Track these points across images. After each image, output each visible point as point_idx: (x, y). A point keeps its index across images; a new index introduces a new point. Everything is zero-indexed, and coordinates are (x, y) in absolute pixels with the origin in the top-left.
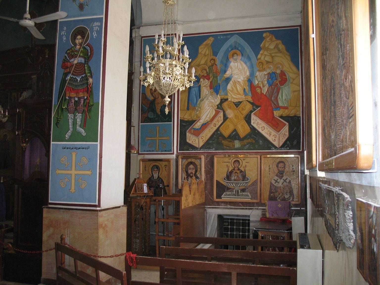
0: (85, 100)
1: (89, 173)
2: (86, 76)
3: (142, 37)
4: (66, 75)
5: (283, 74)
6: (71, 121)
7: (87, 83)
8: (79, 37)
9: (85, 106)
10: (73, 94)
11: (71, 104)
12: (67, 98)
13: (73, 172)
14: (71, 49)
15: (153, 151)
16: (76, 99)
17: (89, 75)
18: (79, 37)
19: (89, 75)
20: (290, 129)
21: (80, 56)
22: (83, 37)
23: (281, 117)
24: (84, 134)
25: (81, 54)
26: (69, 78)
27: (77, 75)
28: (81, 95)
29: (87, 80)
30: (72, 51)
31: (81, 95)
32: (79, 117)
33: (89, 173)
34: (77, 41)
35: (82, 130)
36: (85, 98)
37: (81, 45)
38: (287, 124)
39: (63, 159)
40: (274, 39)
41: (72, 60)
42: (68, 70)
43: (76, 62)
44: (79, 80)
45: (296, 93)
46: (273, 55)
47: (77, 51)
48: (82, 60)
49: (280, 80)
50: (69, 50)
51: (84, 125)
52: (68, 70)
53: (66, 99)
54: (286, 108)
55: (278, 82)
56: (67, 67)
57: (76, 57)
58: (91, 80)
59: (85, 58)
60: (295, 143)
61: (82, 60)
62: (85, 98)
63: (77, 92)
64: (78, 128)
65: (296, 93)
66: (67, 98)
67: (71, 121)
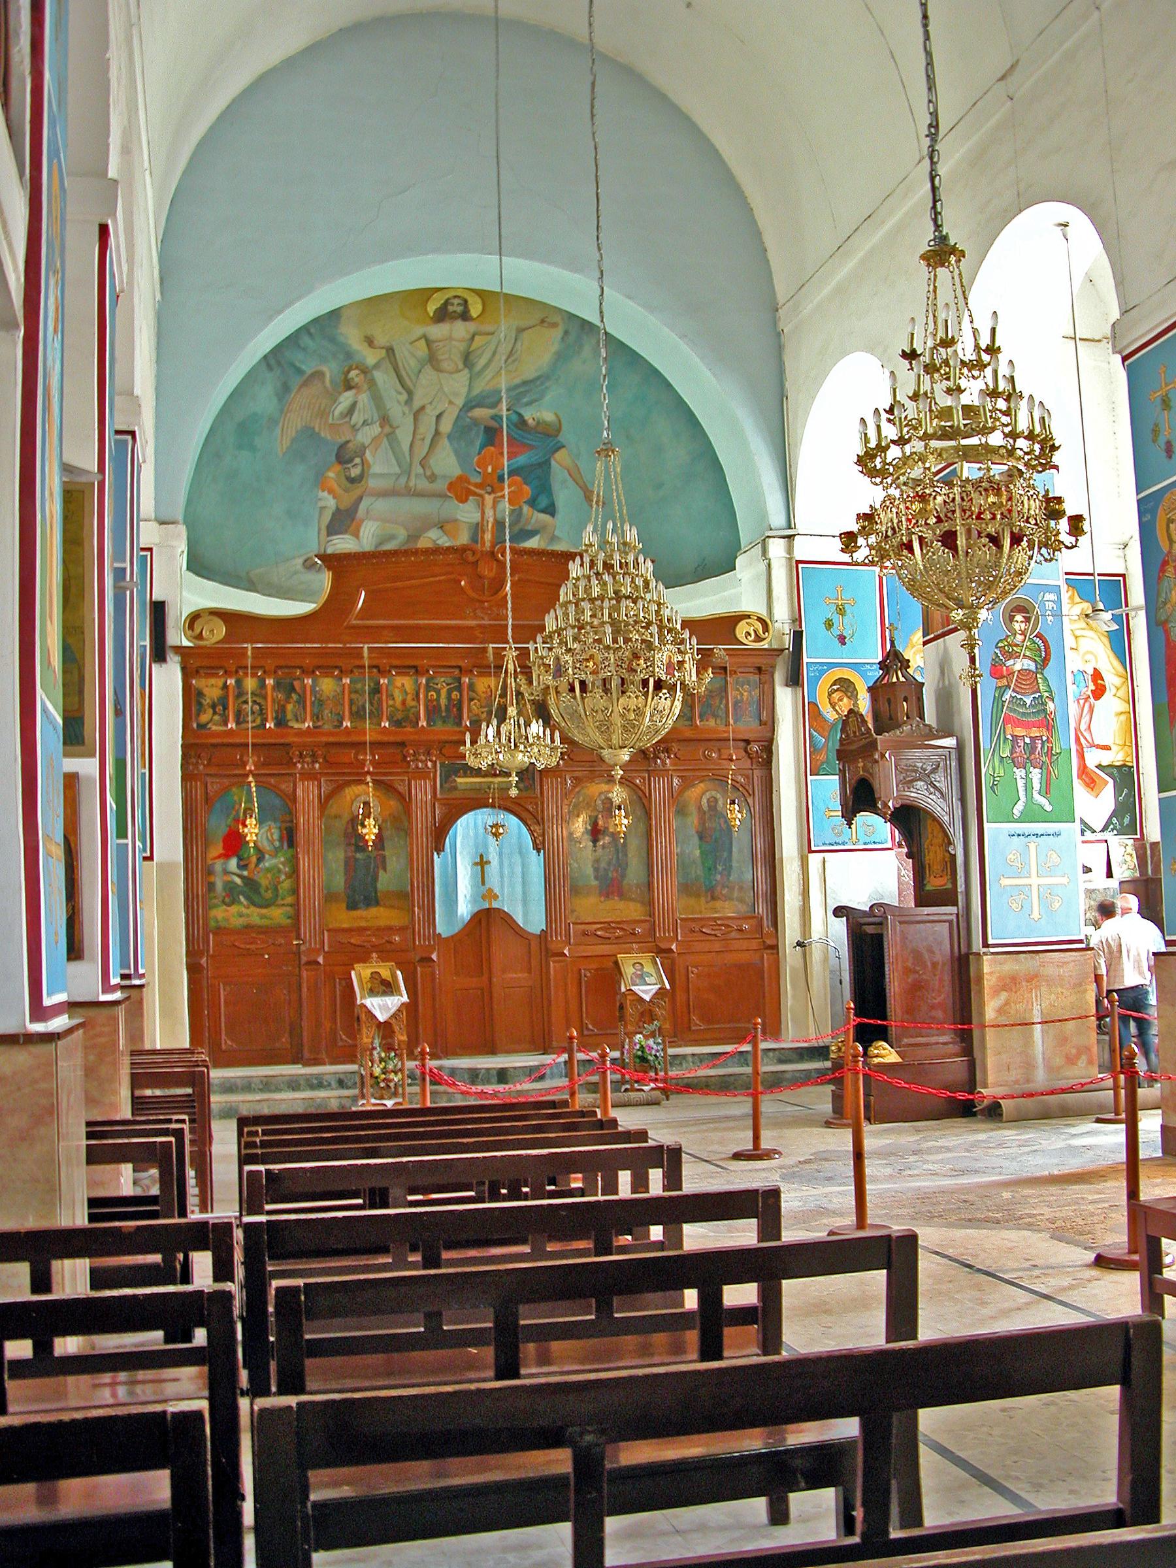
0: (1043, 743)
1: (1064, 880)
2: (1041, 697)
3: (798, 562)
4: (1001, 690)
5: (1097, 675)
6: (1021, 783)
7: (1045, 710)
8: (1019, 617)
9: (1047, 754)
10: (1019, 731)
11: (1018, 750)
12: (1009, 737)
13: (1034, 881)
14: (1006, 639)
15: (844, 843)
16: (1027, 740)
17: (1046, 694)
18: (1019, 617)
19: (1046, 694)
20: (1118, 791)
21: (1025, 657)
22: (1027, 620)
23: (1099, 767)
24: (1048, 808)
25: (1028, 654)
26: (1007, 697)
27: (1022, 694)
28: (1035, 732)
29: (1044, 704)
30: (1009, 645)
31: (1035, 732)
32: (1036, 774)
33: (1064, 880)
34: (1017, 626)
35: (1043, 801)
36: (1044, 738)
37: (1023, 633)
38: (1111, 782)
39: (1011, 856)
40: (1077, 599)
41: (1011, 662)
42: (1005, 682)
43: (1017, 667)
44: (1028, 702)
45: (1123, 717)
46: (1078, 633)
47: (1017, 645)
48: (1032, 666)
49: (1093, 688)
50: (1001, 641)
51: (1046, 790)
52: (1005, 682)
53: (1006, 739)
54: (1107, 748)
55: (1089, 693)
56: (1002, 677)
57: (1018, 657)
58: (1051, 706)
59: (1035, 661)
60: (1126, 821)
61: (1032, 666)
62: (1044, 738)
63: (1027, 726)
64: (1036, 796)
65: (1123, 717)
66: (1009, 737)
67: (1021, 783)
